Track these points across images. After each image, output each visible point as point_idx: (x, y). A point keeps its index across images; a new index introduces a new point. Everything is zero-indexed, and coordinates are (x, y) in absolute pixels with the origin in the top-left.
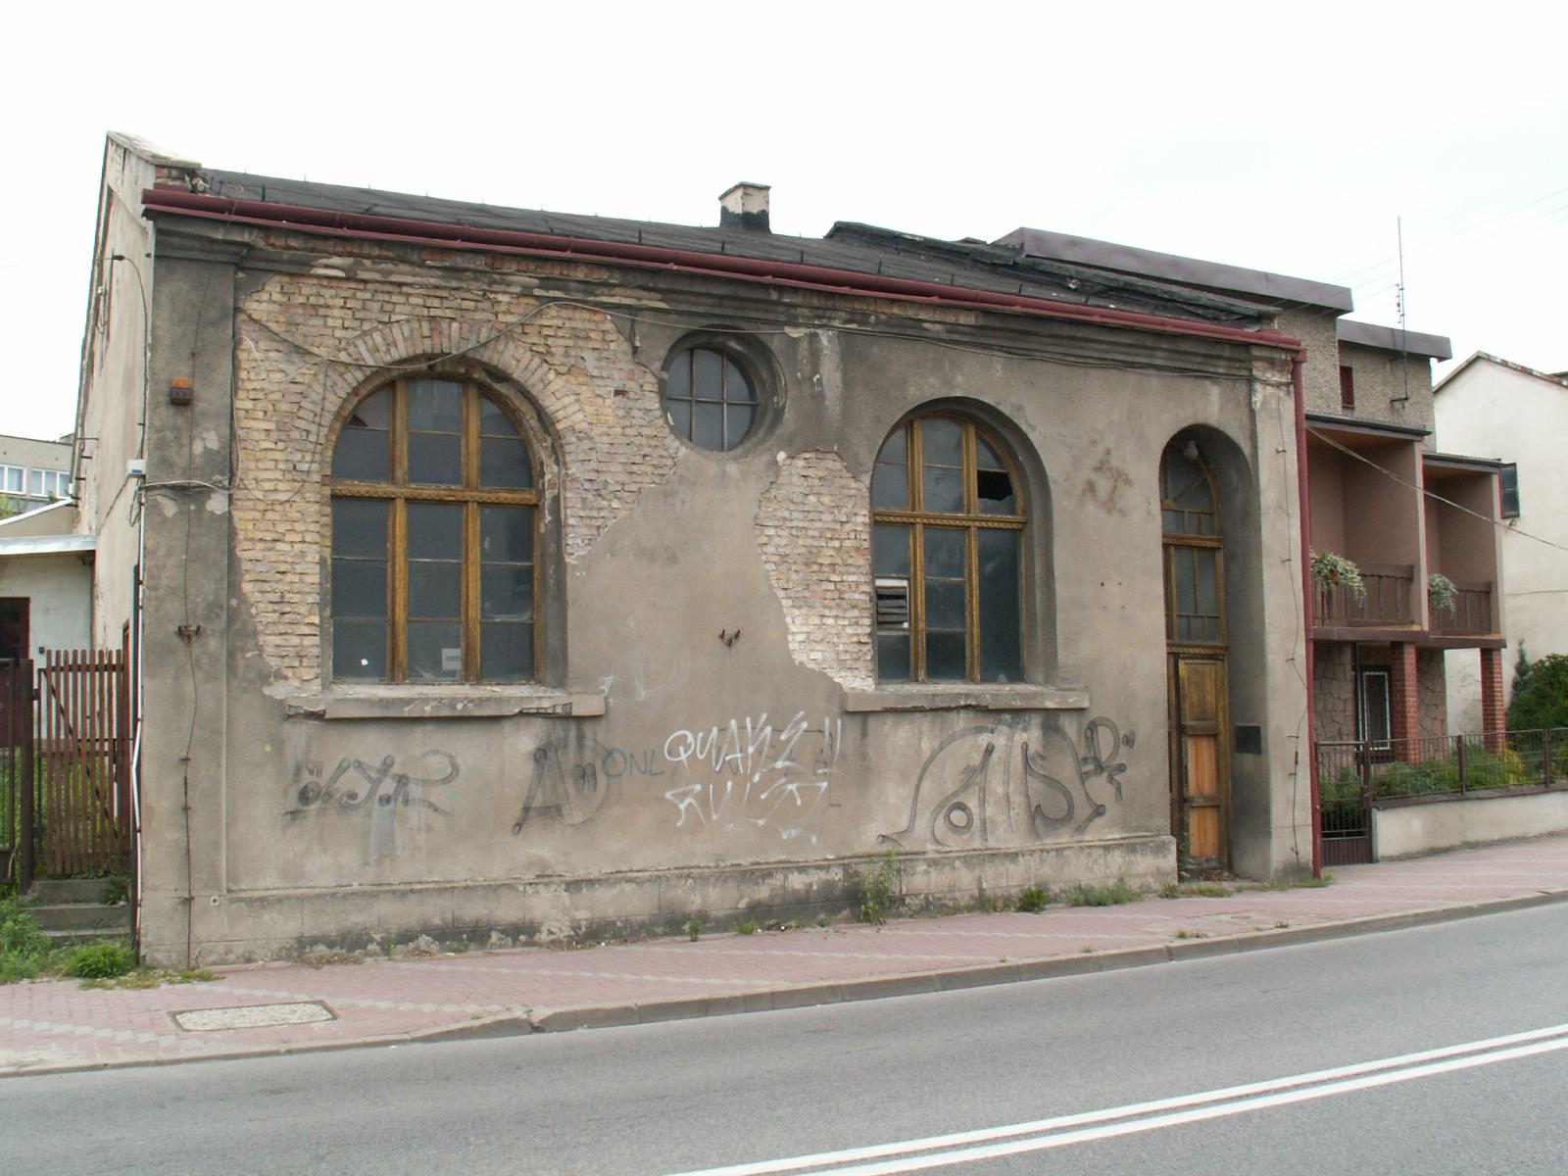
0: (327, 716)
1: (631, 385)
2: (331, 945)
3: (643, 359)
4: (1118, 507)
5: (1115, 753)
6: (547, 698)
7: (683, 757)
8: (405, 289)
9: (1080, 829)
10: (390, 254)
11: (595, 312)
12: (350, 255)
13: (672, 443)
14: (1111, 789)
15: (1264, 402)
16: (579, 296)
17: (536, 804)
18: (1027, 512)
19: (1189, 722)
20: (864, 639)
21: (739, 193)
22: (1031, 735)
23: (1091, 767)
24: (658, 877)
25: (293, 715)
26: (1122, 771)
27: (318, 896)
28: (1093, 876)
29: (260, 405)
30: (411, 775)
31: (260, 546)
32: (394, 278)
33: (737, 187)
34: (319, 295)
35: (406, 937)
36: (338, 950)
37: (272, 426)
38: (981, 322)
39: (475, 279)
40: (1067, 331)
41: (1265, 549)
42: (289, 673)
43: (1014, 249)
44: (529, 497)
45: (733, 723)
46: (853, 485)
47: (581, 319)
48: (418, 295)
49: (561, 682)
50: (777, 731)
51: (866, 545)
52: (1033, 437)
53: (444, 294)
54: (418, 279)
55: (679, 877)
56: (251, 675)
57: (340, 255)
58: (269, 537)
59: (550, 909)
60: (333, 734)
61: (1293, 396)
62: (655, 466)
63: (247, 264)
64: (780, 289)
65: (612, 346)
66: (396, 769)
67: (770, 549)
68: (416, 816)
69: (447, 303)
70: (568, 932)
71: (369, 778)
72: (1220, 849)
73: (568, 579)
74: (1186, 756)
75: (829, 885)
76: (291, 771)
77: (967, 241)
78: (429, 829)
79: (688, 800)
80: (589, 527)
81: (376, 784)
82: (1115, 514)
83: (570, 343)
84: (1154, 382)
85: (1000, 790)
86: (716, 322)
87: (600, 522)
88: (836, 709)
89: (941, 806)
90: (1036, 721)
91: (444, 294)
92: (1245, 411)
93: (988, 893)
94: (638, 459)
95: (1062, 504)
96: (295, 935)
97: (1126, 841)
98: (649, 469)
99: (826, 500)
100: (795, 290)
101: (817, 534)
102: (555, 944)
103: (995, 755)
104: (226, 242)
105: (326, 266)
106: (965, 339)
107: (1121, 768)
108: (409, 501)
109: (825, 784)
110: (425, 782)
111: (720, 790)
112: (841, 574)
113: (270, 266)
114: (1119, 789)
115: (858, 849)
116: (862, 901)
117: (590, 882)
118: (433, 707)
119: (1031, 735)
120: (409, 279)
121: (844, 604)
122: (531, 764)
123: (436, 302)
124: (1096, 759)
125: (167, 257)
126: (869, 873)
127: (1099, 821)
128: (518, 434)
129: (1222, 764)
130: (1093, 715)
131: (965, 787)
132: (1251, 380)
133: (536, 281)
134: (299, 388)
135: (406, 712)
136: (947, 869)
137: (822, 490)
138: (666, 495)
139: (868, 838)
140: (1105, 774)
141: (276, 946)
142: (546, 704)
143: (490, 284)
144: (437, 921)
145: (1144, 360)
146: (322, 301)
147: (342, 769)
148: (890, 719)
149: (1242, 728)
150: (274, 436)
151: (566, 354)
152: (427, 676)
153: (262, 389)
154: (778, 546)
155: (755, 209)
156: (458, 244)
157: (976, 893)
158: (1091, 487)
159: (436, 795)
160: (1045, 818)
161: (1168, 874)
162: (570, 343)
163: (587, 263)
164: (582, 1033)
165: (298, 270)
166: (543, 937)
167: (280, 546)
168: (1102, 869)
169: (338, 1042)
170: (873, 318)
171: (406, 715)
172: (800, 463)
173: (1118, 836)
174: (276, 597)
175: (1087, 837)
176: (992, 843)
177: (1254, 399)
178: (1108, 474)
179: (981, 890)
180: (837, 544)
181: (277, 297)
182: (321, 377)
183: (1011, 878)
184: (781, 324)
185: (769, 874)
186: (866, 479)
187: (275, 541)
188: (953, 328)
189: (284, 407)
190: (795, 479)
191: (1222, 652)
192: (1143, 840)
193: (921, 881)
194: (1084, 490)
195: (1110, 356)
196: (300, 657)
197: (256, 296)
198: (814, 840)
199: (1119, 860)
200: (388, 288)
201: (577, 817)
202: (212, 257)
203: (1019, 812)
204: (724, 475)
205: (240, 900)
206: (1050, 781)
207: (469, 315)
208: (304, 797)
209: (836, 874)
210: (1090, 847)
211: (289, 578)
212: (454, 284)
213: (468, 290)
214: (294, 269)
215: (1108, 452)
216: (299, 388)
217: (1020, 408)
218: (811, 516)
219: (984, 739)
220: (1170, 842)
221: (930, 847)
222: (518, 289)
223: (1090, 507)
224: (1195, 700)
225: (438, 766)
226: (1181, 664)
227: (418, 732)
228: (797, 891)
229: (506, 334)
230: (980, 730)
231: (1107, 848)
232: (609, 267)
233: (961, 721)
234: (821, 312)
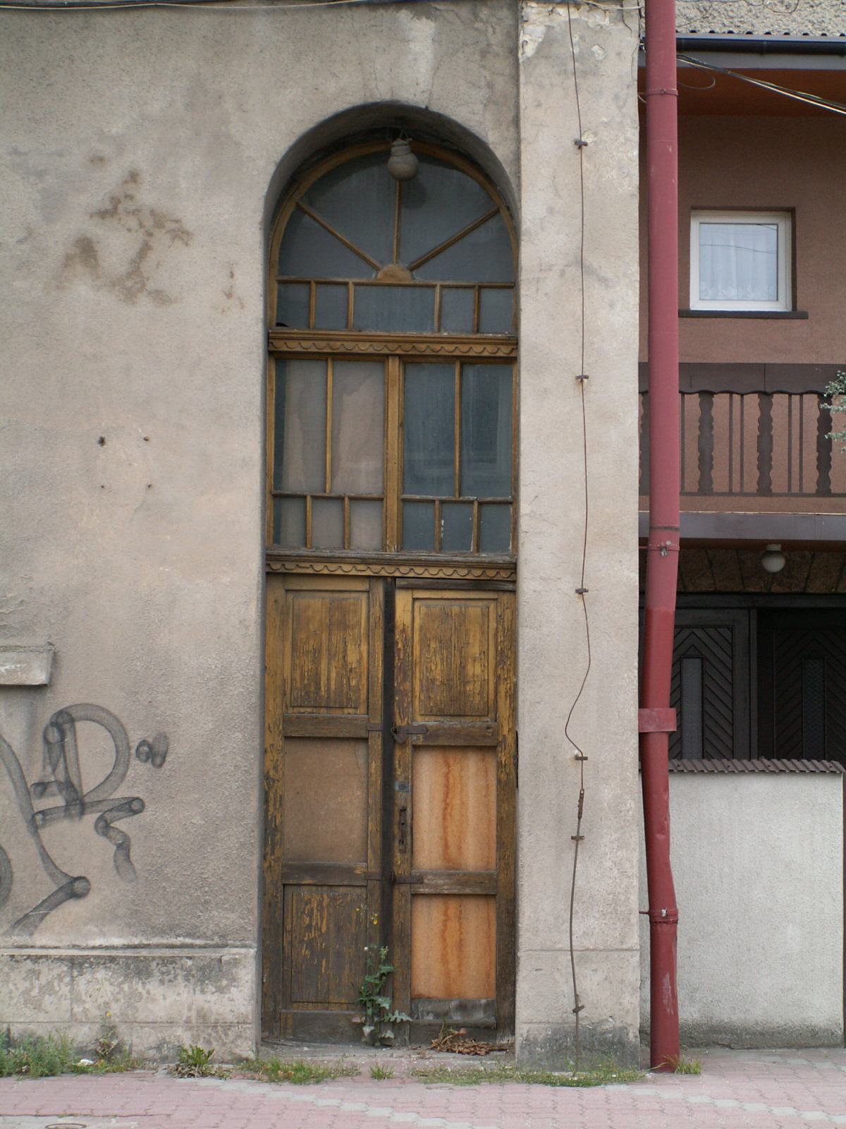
4: (150, 285)
9: (25, 922)
14: (106, 848)
15: (548, 42)
23: (59, 801)
26: (135, 812)
28: (42, 1017)
61: (636, 24)
82: (145, 304)
92: (503, 65)
97: (129, 953)
107: (132, 807)
114: (124, 847)
124: (69, 786)
127: (73, 908)
130: (66, 696)
140: (91, 818)
158: (86, 250)
161: (231, 1025)
168: (66, 1004)
173: (117, 941)
175: (41, 939)
177: (522, 38)
178: (132, 222)
191: (504, 575)
192: (168, 953)
194: (68, 260)
199: (108, 990)
210: (36, 959)
215: (134, 177)
220: (235, 962)
223: (82, 290)
224: (438, 672)
226: (402, 600)
231: (76, 964)
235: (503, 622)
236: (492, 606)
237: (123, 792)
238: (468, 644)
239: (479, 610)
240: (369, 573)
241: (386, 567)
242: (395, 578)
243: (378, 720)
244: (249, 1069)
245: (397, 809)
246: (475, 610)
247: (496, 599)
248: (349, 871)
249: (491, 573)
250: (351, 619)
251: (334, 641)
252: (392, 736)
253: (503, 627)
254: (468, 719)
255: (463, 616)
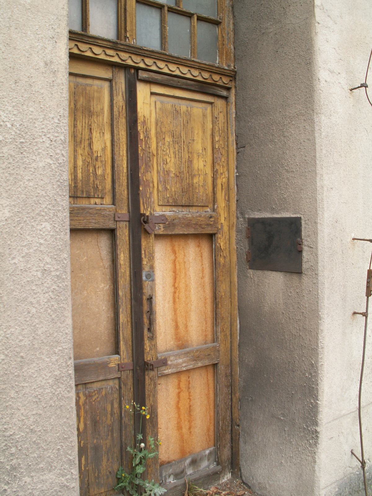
19: (156, 208)
72: (218, 439)
74: (151, 276)
129: (223, 288)
149: (263, 221)
224: (172, 166)
235: (218, 123)
236: (209, 108)
238: (194, 140)
239: (200, 110)
240: (116, 59)
241: (134, 57)
242: (137, 69)
243: (124, 211)
245: (145, 298)
246: (197, 110)
247: (212, 103)
248: (104, 366)
249: (216, 78)
250: (95, 107)
251: (79, 127)
252: (140, 225)
253: (219, 127)
254: (194, 210)
255: (189, 114)
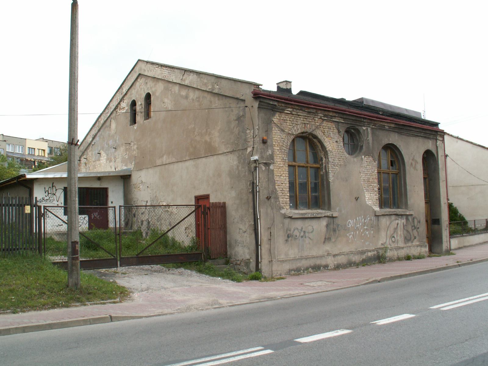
0: (293, 217)
1: (338, 140)
2: (295, 271)
3: (340, 134)
5: (417, 225)
6: (329, 213)
7: (350, 226)
8: (300, 116)
9: (412, 242)
10: (299, 108)
11: (332, 123)
12: (292, 108)
13: (346, 153)
16: (329, 119)
17: (327, 237)
18: (399, 169)
20: (377, 199)
21: (285, 83)
22: (404, 221)
23: (413, 228)
24: (348, 254)
25: (285, 217)
27: (292, 260)
29: (277, 143)
30: (306, 231)
31: (278, 177)
32: (299, 114)
33: (284, 82)
34: (285, 117)
35: (307, 269)
36: (296, 272)
37: (279, 148)
38: (395, 126)
39: (312, 115)
40: (409, 128)
41: (440, 178)
42: (284, 207)
43: (360, 102)
44: (318, 166)
45: (358, 218)
46: (374, 163)
47: (330, 124)
48: (302, 118)
49: (329, 209)
50: (365, 220)
51: (377, 177)
52: (403, 153)
53: (306, 118)
54: (303, 114)
55: (351, 253)
56: (278, 208)
57: (290, 108)
58: (280, 175)
59: (331, 261)
60: (293, 222)
62: (343, 159)
63: (274, 110)
64: (364, 118)
65: (335, 131)
66: (303, 230)
67: (362, 178)
68: (307, 240)
69: (307, 120)
70: (334, 267)
71: (299, 232)
73: (330, 185)
75: (374, 255)
76: (286, 231)
77: (342, 99)
78: (309, 243)
79: (351, 236)
80: (333, 173)
81: (300, 233)
83: (328, 130)
84: (421, 140)
85: (400, 233)
86: (352, 125)
87: (334, 172)
88: (374, 215)
89: (390, 237)
90: (405, 217)
91: (306, 118)
92: (435, 147)
93: (399, 257)
94: (340, 157)
95: (407, 167)
96: (289, 269)
98: (342, 160)
99: (370, 167)
100: (366, 118)
101: (369, 175)
102: (331, 270)
103: (399, 225)
104: (272, 104)
105: (287, 111)
106: (391, 130)
107: (418, 228)
108: (299, 166)
109: (372, 232)
110: (308, 233)
111: (356, 234)
112: (373, 184)
113: (277, 110)
115: (378, 247)
116: (380, 259)
117: (337, 255)
118: (311, 215)
119: (404, 221)
120: (301, 114)
121: (374, 191)
122: (326, 228)
123: (305, 120)
124: (414, 226)
125: (260, 107)
126: (381, 252)
127: (415, 240)
128: (315, 150)
130: (413, 216)
131: (394, 232)
132: (436, 139)
133: (323, 115)
134: (283, 139)
135: (306, 216)
136: (393, 251)
137: (370, 165)
138: (345, 166)
139: (379, 245)
141: (285, 272)
142: (329, 214)
143: (315, 116)
144: (312, 265)
145: (419, 135)
146: (286, 119)
147: (294, 230)
148: (382, 217)
150: (279, 151)
151: (328, 133)
152: (302, 208)
153: (277, 140)
154: (363, 178)
155: (289, 88)
156: (312, 106)
157: (397, 256)
158: (412, 164)
159: (311, 235)
160: (407, 239)
162: (328, 130)
163: (332, 112)
164: (385, 283)
165: (281, 111)
166: (329, 268)
167: (281, 177)
169: (346, 287)
170: (377, 125)
171: (306, 217)
172: (366, 158)
173: (418, 243)
174: (281, 189)
176: (399, 245)
179: (398, 256)
180: (372, 177)
181: (278, 118)
182: (287, 137)
183: (402, 253)
184: (362, 126)
185: (365, 253)
186: (377, 162)
187: (281, 176)
188: (390, 127)
189: (281, 144)
190: (365, 162)
193: (389, 254)
195: (413, 134)
196: (286, 203)
197: (274, 117)
198: (371, 244)
200: (297, 116)
201: (333, 240)
202: (269, 108)
203: (403, 237)
204: (354, 161)
205: (279, 261)
206: (408, 231)
207: (311, 123)
208: (288, 237)
209: (375, 253)
211: (283, 185)
212: (308, 116)
213: (311, 117)
214: (281, 111)
216: (283, 139)
217: (400, 146)
218: (368, 171)
219: (397, 221)
221: (389, 246)
222: (319, 117)
225: (310, 228)
227: (307, 221)
228: (369, 256)
229: (317, 127)
230: (396, 219)
232: (336, 112)
233: (393, 217)
234: (368, 123)
237: (417, 227)
244: (429, 256)
